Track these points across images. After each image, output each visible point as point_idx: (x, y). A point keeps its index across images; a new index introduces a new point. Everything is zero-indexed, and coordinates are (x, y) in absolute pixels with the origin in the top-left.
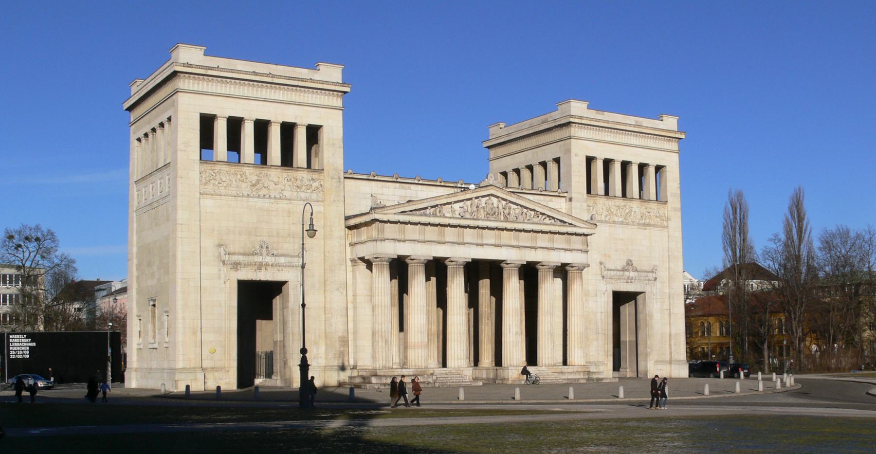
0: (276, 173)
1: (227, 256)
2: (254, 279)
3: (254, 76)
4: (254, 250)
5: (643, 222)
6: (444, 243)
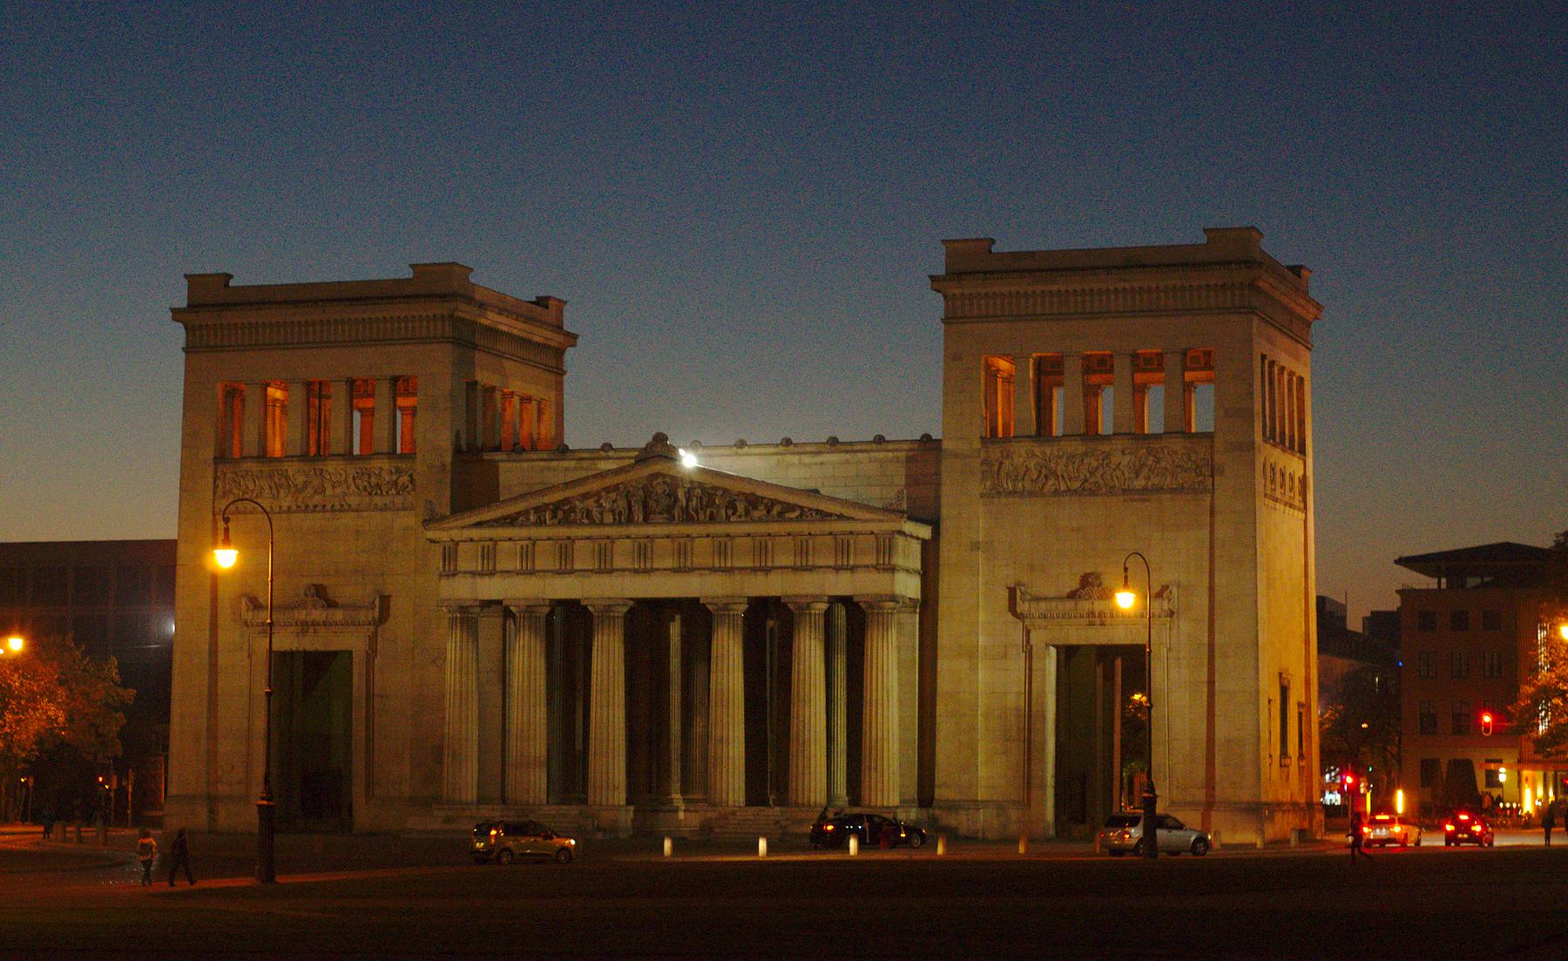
5: (1140, 483)
6: (572, 572)
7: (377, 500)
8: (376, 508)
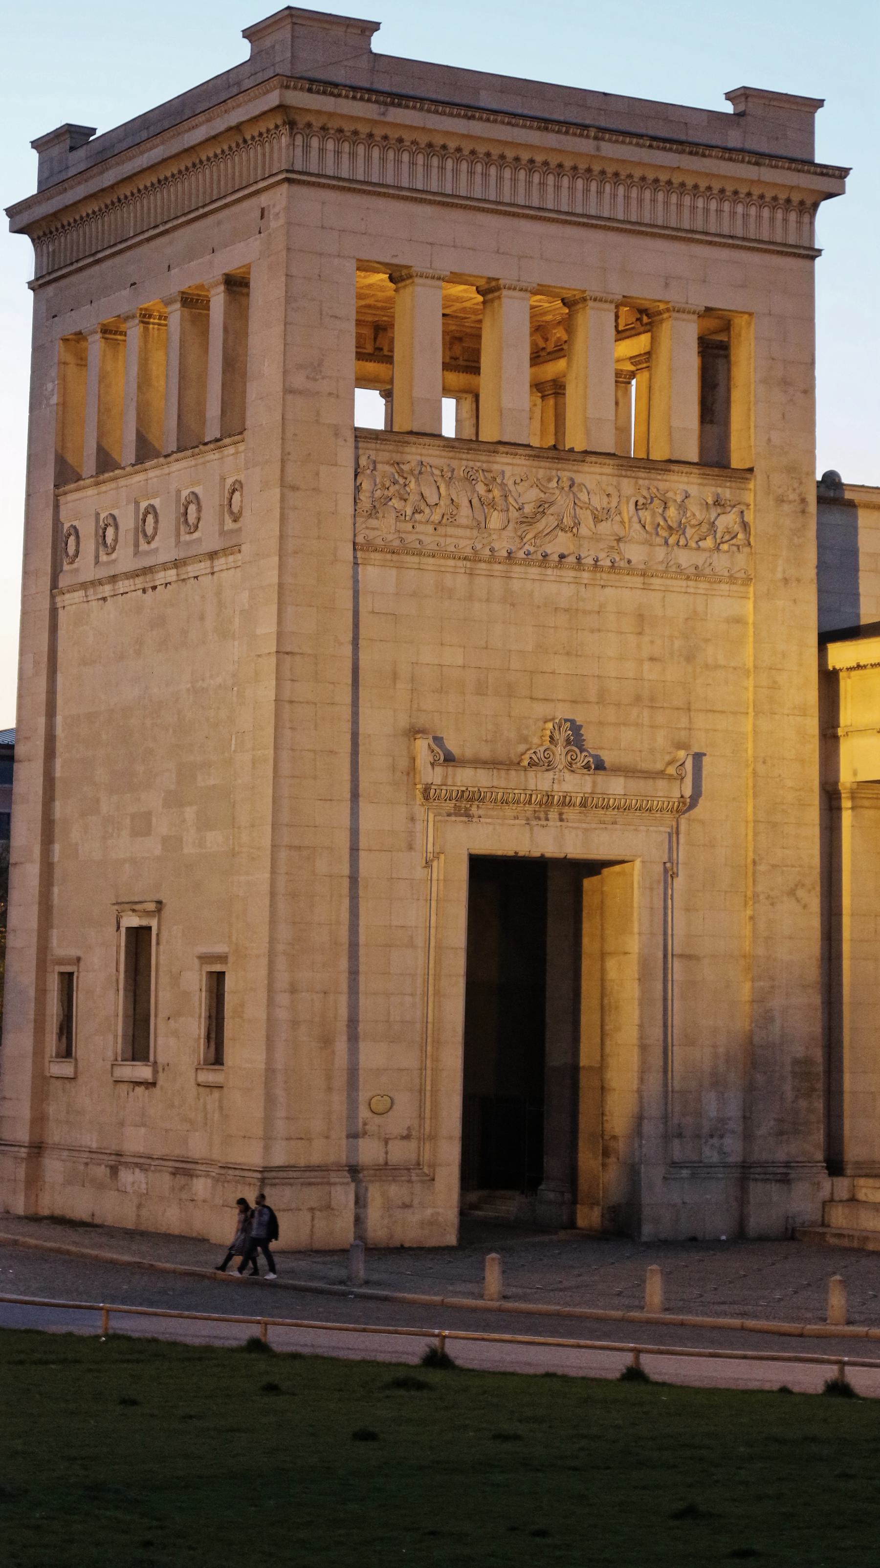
0: (598, 477)
1: (439, 770)
2: (521, 854)
3: (538, 133)
4: (522, 748)
7: (684, 558)
8: (680, 573)
